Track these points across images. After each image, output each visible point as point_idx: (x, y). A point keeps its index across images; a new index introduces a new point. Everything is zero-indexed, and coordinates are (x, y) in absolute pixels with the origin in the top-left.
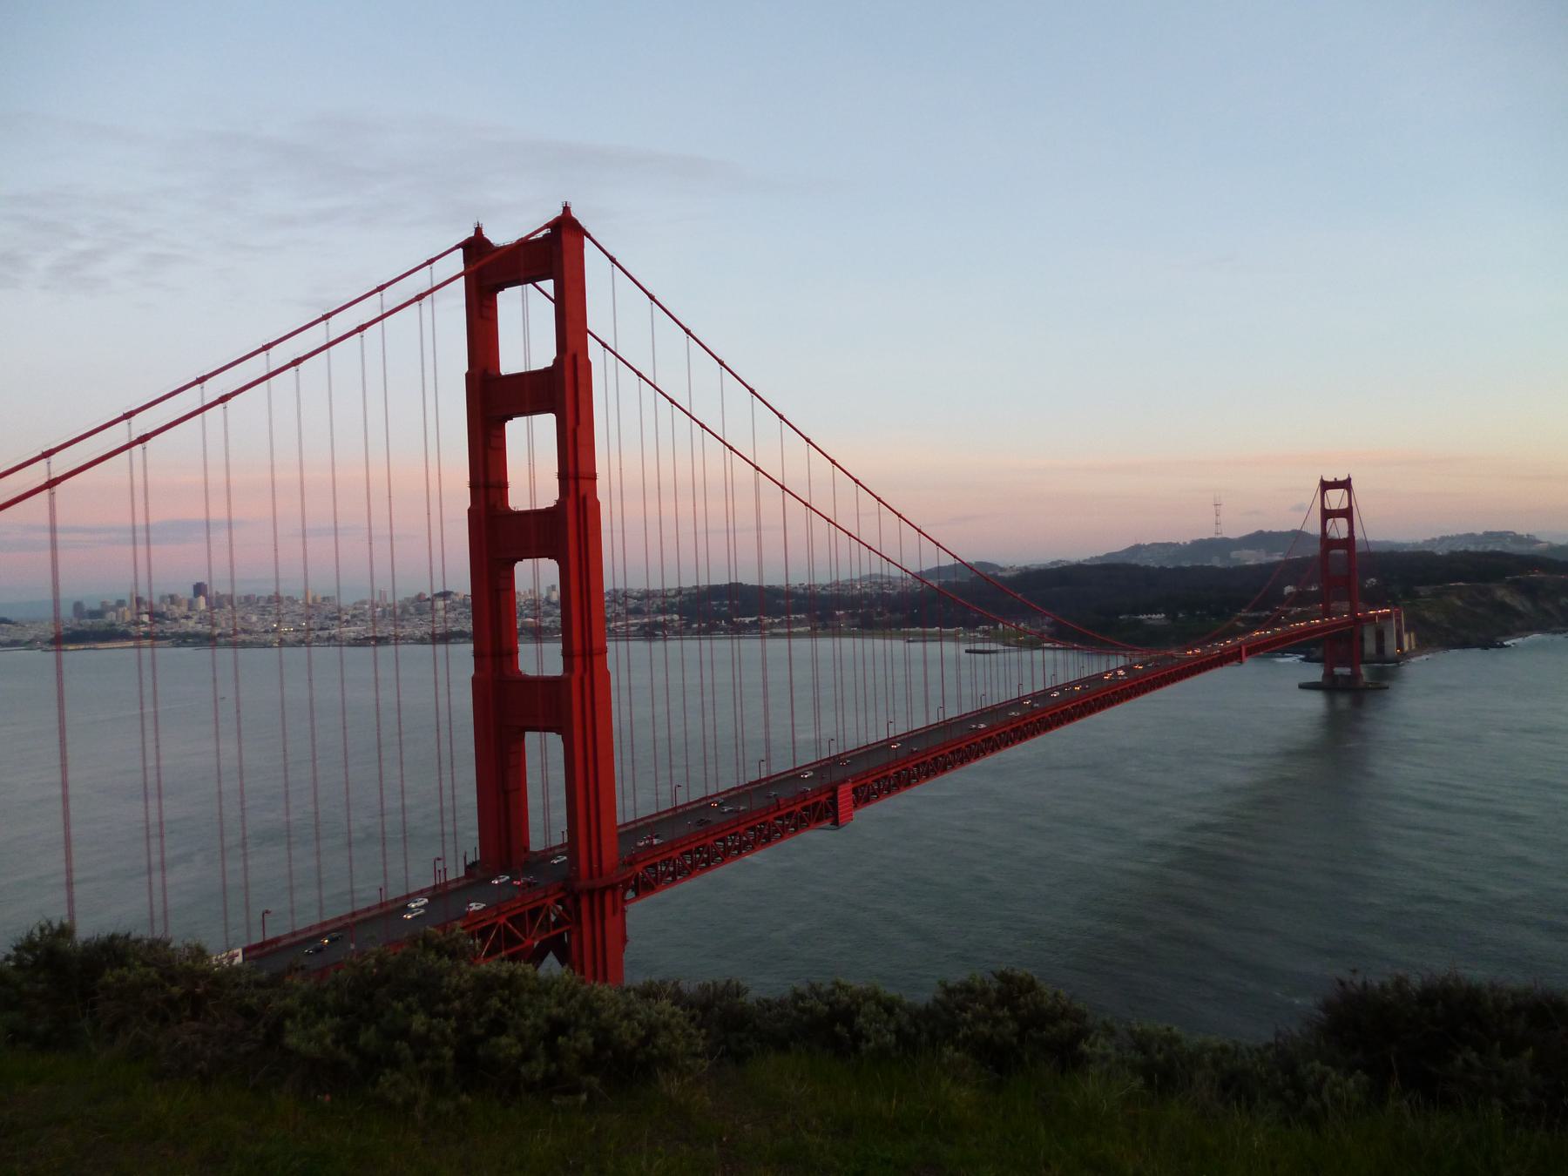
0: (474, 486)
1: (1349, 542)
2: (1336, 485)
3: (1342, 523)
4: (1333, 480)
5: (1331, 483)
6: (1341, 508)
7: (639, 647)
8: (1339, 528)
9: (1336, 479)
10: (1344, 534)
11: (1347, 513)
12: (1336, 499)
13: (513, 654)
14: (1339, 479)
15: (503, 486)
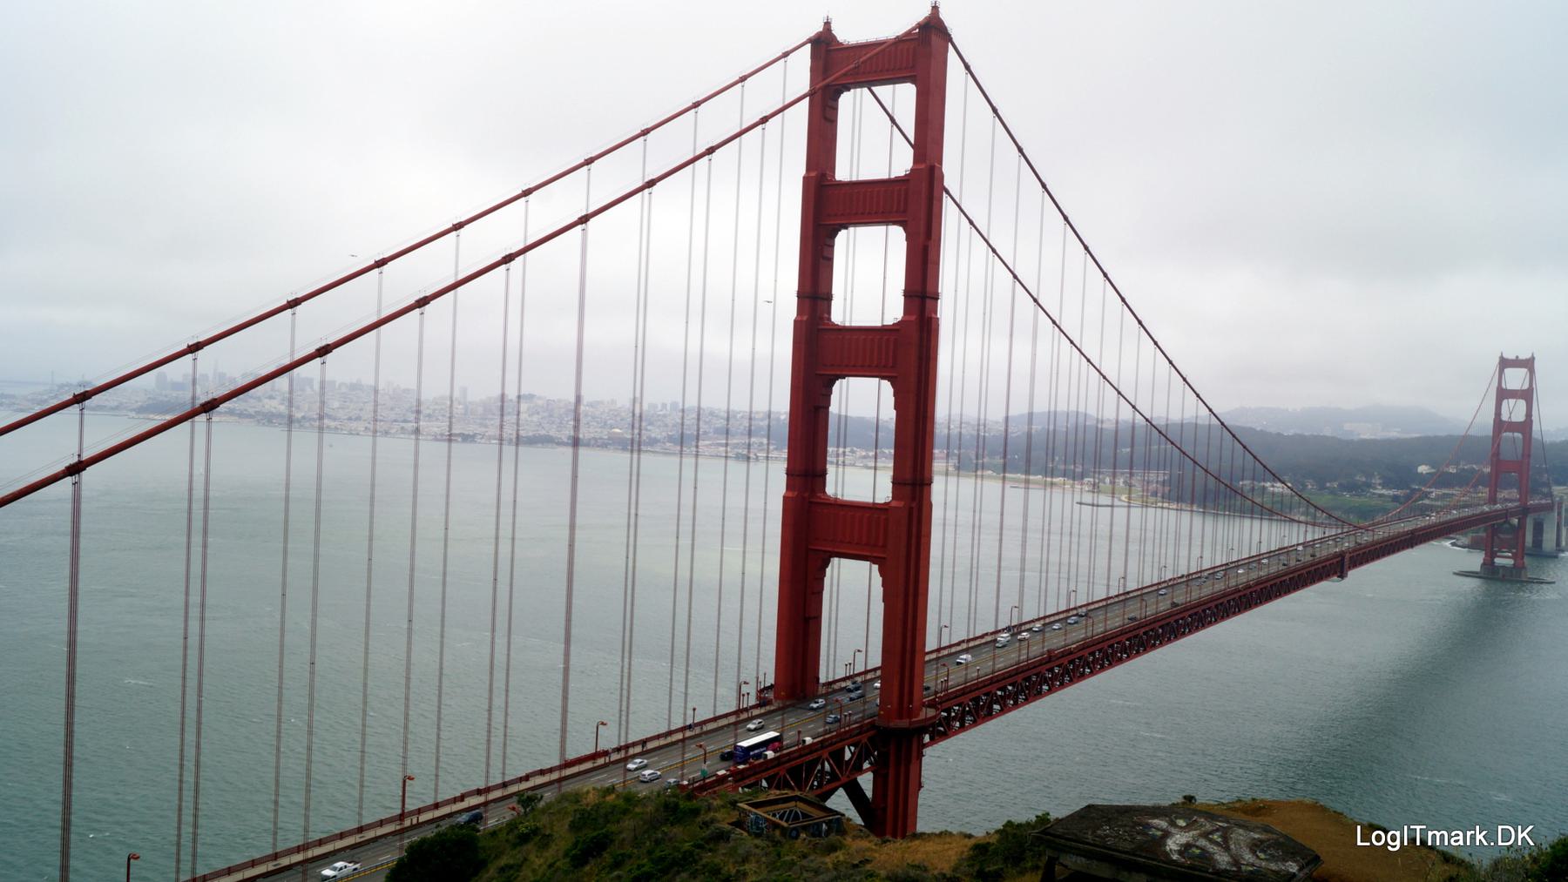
0: (801, 295)
1: (1526, 427)
2: (1517, 363)
3: (1521, 405)
4: (1514, 358)
5: (1512, 360)
6: (1523, 388)
7: (967, 484)
8: (1515, 411)
9: (1517, 357)
10: (1519, 416)
11: (1527, 395)
12: (1515, 379)
13: (823, 474)
14: (1521, 357)
15: (828, 298)
